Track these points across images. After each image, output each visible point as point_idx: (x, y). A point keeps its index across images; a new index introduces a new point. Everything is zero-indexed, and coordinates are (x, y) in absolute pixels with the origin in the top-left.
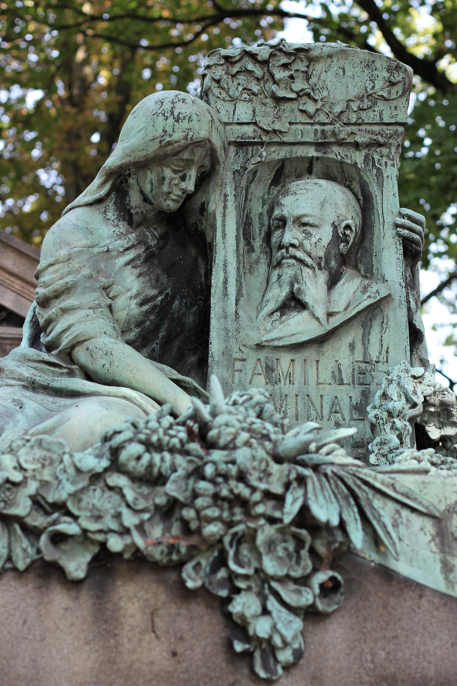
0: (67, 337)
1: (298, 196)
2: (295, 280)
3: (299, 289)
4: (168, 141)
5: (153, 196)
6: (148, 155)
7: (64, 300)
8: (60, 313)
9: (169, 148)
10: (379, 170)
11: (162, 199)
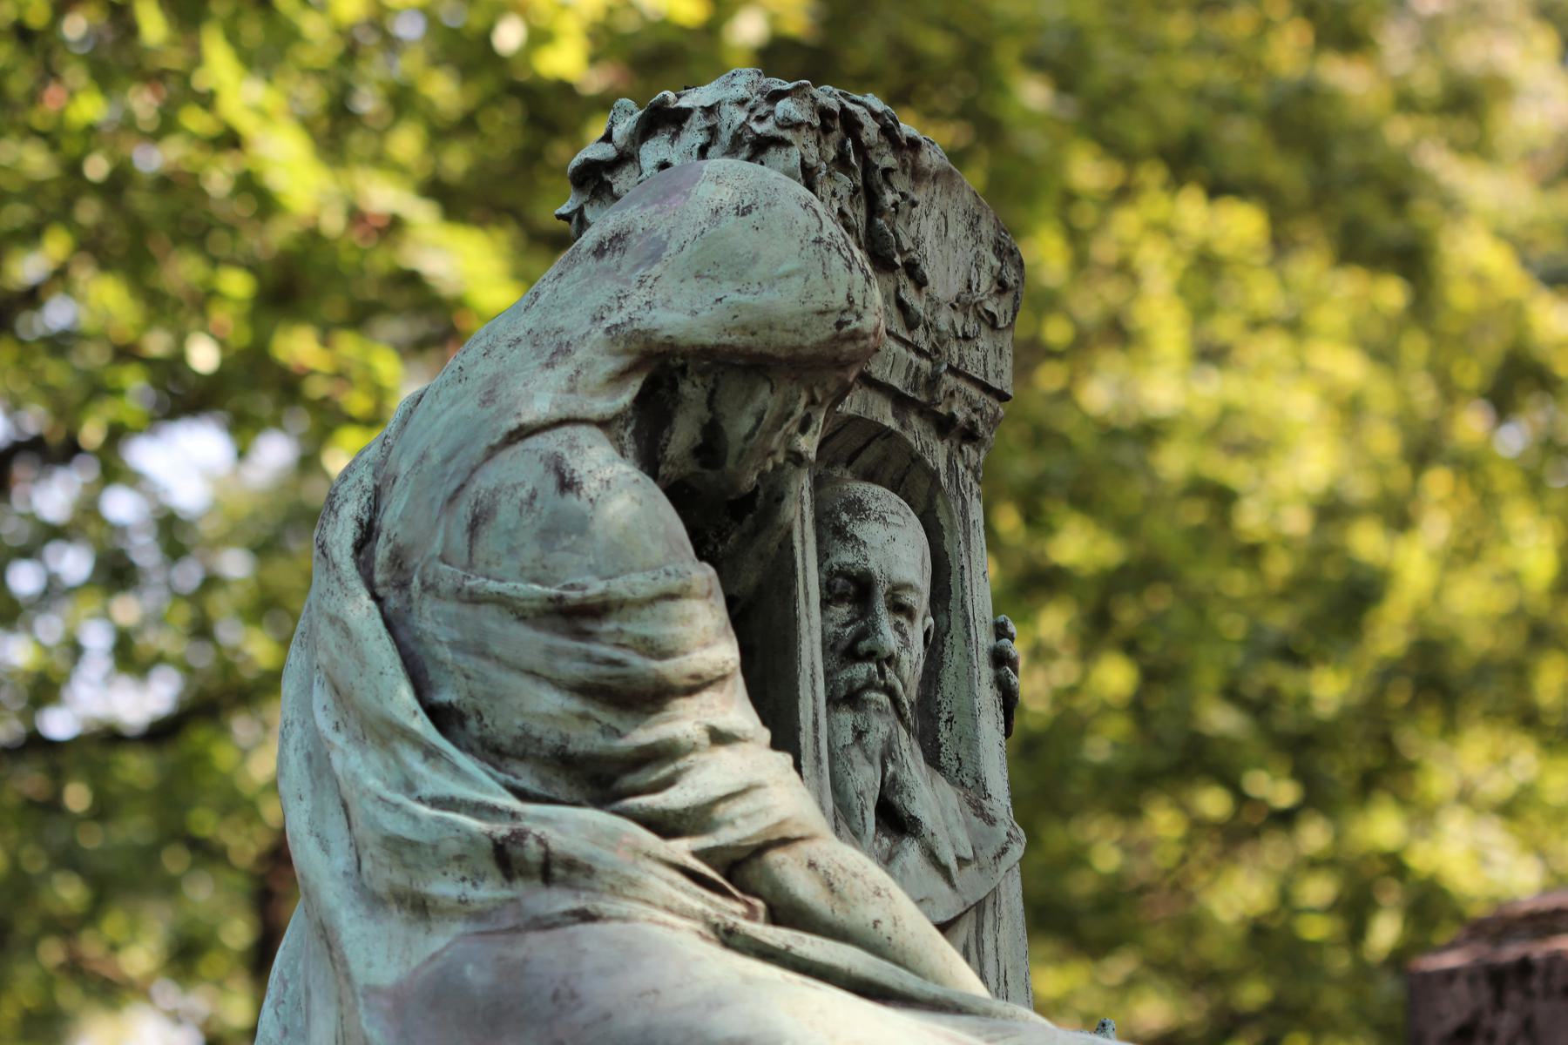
0: (746, 816)
1: (893, 531)
2: (888, 753)
3: (894, 778)
4: (856, 330)
5: (741, 454)
6: (801, 347)
7: (712, 706)
8: (704, 739)
9: (849, 347)
10: (964, 499)
11: (752, 465)
